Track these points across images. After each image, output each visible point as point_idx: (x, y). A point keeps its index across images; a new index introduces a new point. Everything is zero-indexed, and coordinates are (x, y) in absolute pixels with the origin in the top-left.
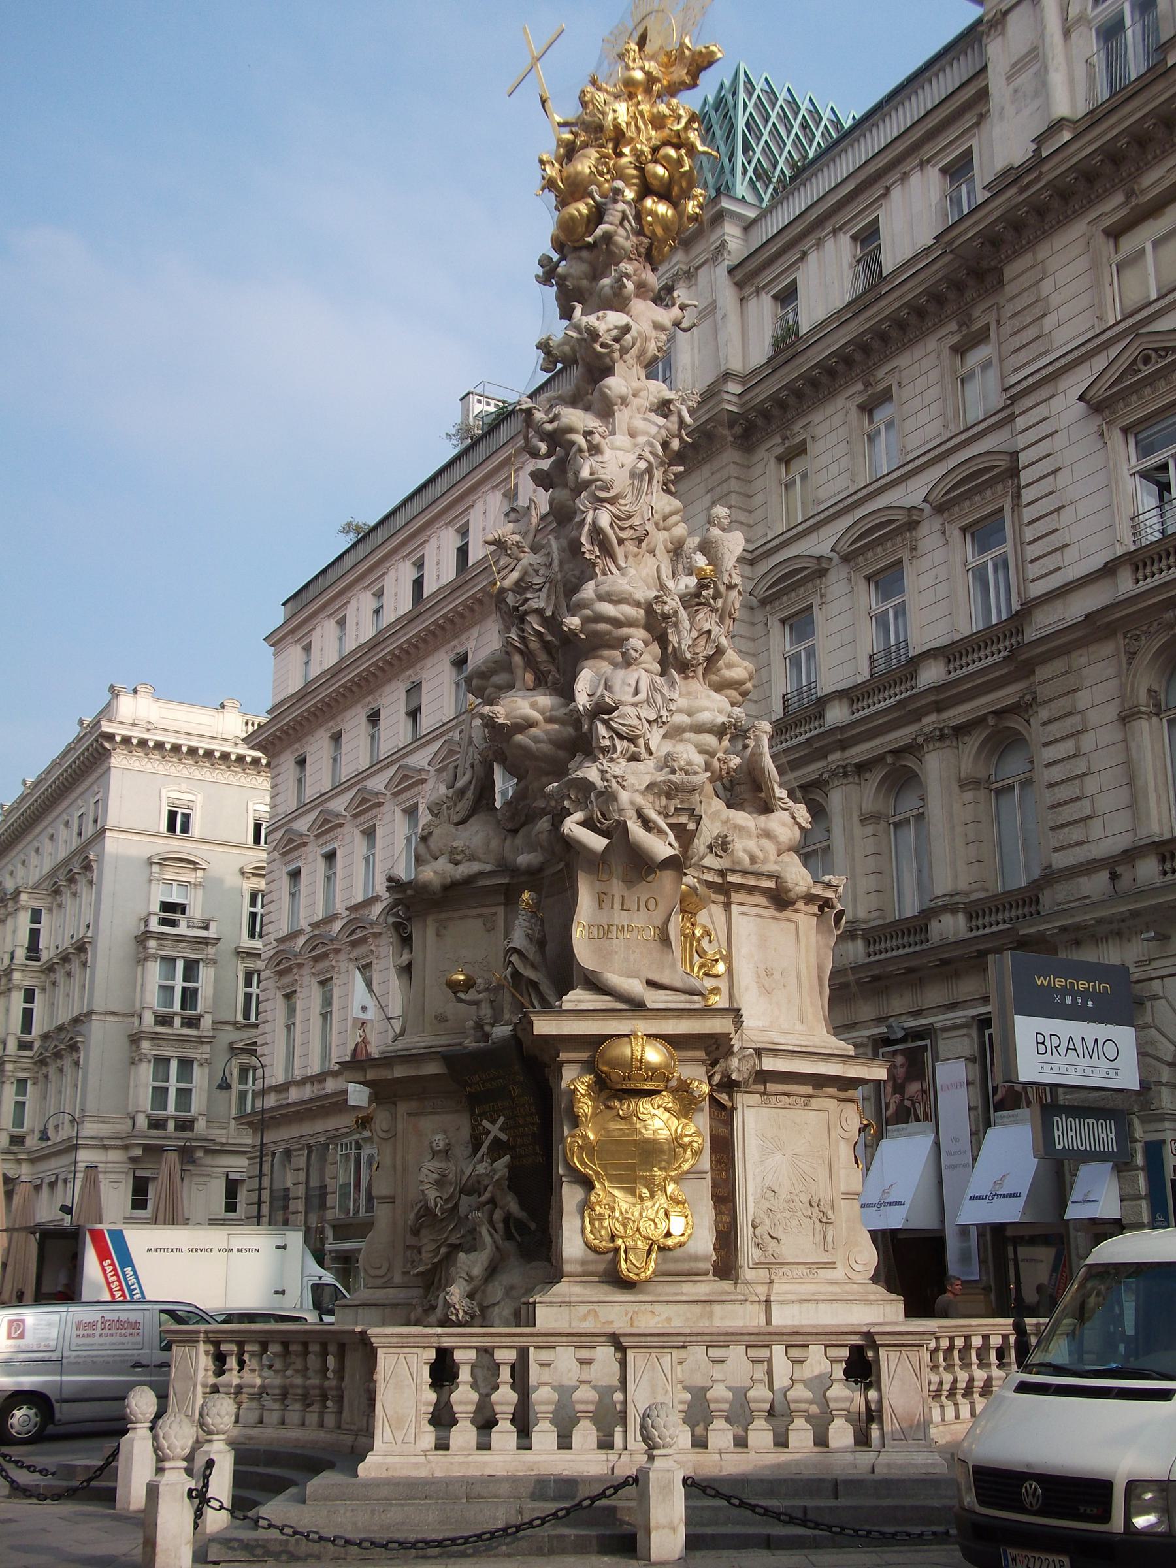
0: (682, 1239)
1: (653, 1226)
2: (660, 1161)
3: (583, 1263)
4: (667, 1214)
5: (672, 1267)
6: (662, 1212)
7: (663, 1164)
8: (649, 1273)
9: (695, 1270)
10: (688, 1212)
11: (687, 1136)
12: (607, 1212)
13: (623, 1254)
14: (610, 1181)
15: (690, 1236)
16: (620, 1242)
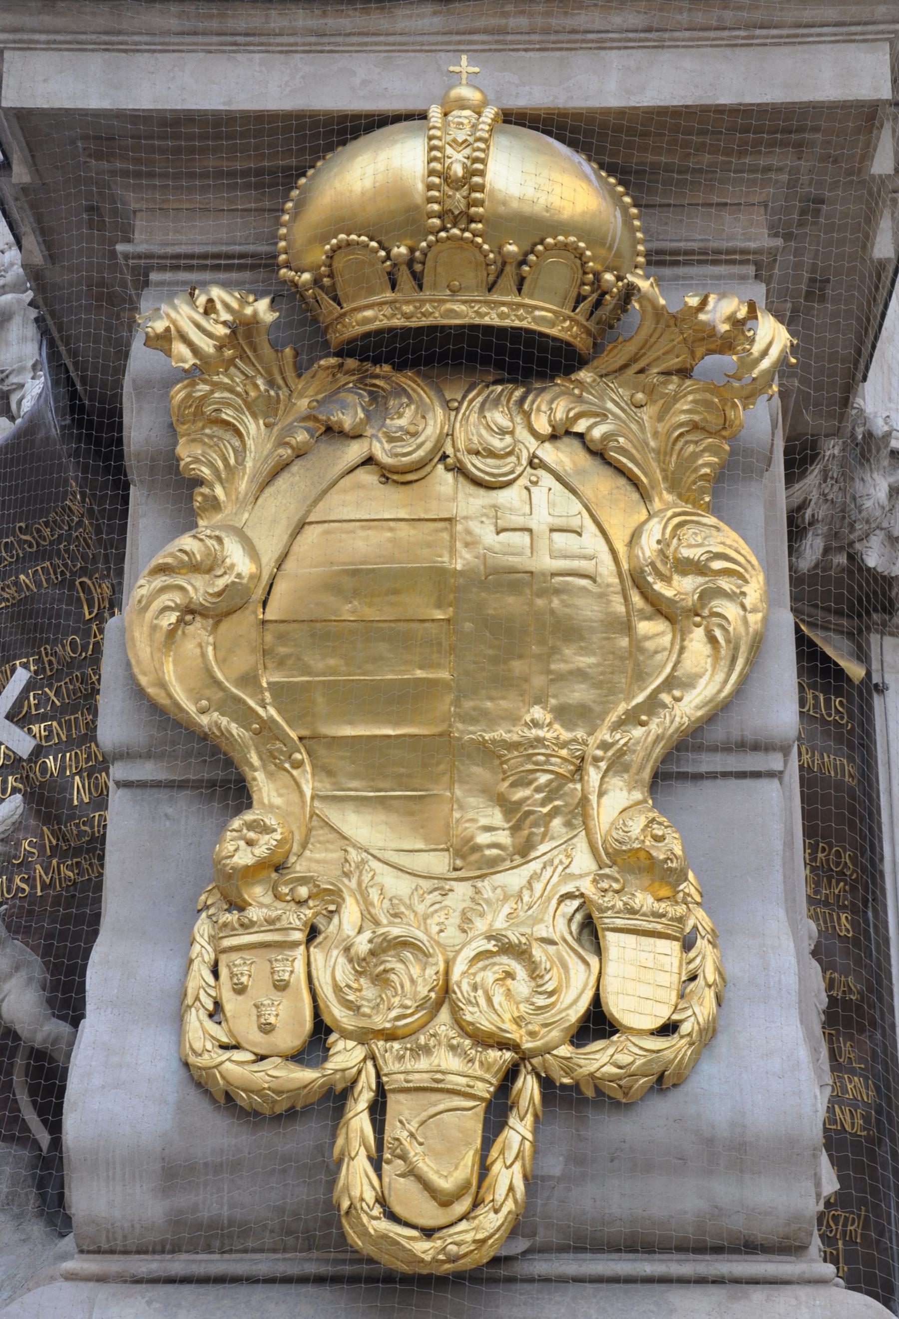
0: (674, 1048)
1: (522, 985)
2: (560, 678)
3: (174, 1173)
4: (590, 931)
5: (615, 1199)
6: (559, 924)
7: (579, 694)
8: (490, 1221)
9: (737, 1224)
10: (699, 918)
11: (687, 567)
12: (295, 920)
13: (359, 1120)
14: (322, 769)
15: (708, 1035)
16: (345, 1056)
